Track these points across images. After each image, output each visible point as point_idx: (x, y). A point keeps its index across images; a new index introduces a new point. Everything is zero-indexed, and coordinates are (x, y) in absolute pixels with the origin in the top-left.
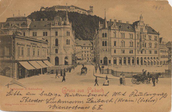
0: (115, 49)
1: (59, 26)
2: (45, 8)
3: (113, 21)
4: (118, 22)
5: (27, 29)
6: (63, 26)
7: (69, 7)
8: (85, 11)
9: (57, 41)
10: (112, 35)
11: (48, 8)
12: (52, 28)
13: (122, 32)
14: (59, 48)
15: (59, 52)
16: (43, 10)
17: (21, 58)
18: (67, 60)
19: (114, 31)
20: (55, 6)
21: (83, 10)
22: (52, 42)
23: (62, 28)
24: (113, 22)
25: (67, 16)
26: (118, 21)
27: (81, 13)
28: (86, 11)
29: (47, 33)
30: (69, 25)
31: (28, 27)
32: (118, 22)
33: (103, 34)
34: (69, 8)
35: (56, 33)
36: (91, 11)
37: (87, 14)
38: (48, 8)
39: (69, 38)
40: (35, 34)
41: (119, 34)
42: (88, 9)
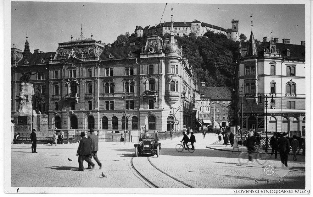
1: (157, 56)
2: (144, 28)
3: (268, 40)
4: (282, 42)
5: (95, 62)
6: (163, 55)
8: (223, 30)
11: (150, 27)
12: (142, 59)
13: (291, 63)
14: (156, 97)
15: (156, 105)
20: (162, 24)
23: (162, 58)
24: (269, 44)
26: (280, 41)
28: (223, 30)
32: (282, 42)
34: (191, 25)
36: (235, 30)
38: (148, 27)
41: (282, 67)
42: (229, 26)
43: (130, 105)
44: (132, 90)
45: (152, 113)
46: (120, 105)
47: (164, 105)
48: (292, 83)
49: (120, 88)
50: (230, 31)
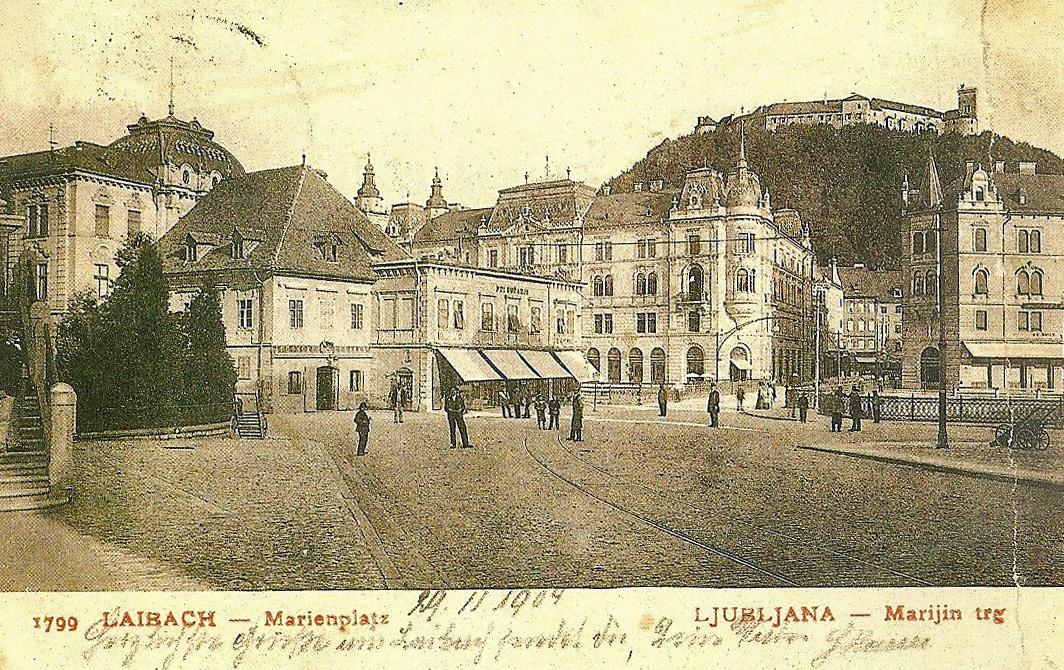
0: (983, 308)
5: (572, 230)
6: (722, 211)
7: (837, 105)
9: (696, 273)
10: (965, 237)
12: (677, 222)
14: (705, 306)
15: (704, 325)
16: (707, 129)
17: (452, 336)
18: (741, 364)
19: (975, 219)
21: (922, 111)
22: (675, 281)
23: (719, 218)
25: (744, 164)
27: (908, 126)
29: (652, 243)
30: (751, 204)
31: (578, 224)
33: (918, 236)
35: (695, 243)
37: (939, 126)
39: (749, 263)
40: (605, 251)
41: (1003, 232)
42: (949, 102)
43: (646, 324)
44: (653, 292)
45: (696, 340)
46: (625, 322)
47: (724, 323)
48: (1033, 271)
49: (624, 286)
50: (947, 116)
